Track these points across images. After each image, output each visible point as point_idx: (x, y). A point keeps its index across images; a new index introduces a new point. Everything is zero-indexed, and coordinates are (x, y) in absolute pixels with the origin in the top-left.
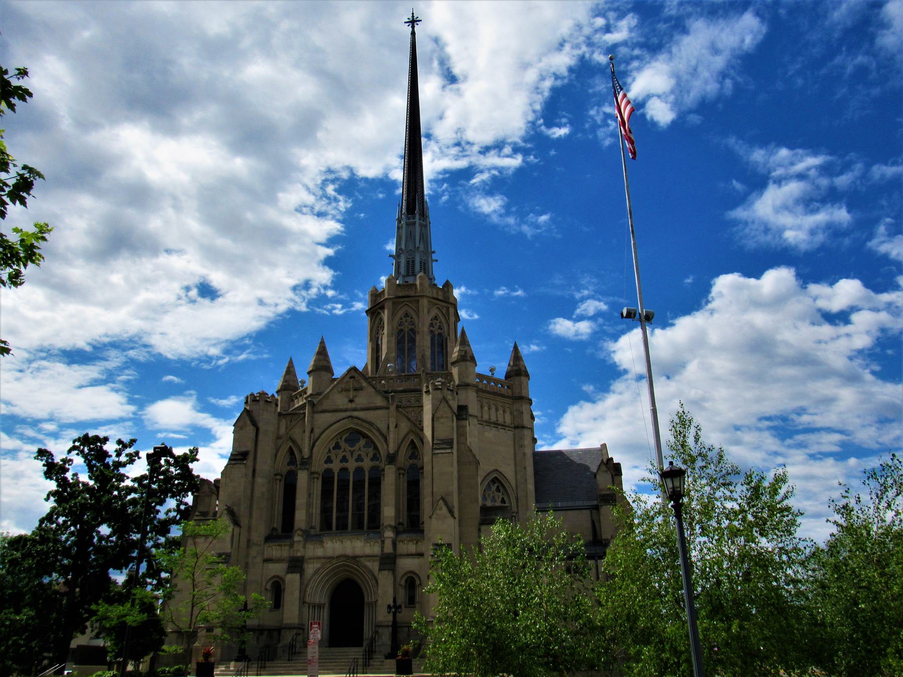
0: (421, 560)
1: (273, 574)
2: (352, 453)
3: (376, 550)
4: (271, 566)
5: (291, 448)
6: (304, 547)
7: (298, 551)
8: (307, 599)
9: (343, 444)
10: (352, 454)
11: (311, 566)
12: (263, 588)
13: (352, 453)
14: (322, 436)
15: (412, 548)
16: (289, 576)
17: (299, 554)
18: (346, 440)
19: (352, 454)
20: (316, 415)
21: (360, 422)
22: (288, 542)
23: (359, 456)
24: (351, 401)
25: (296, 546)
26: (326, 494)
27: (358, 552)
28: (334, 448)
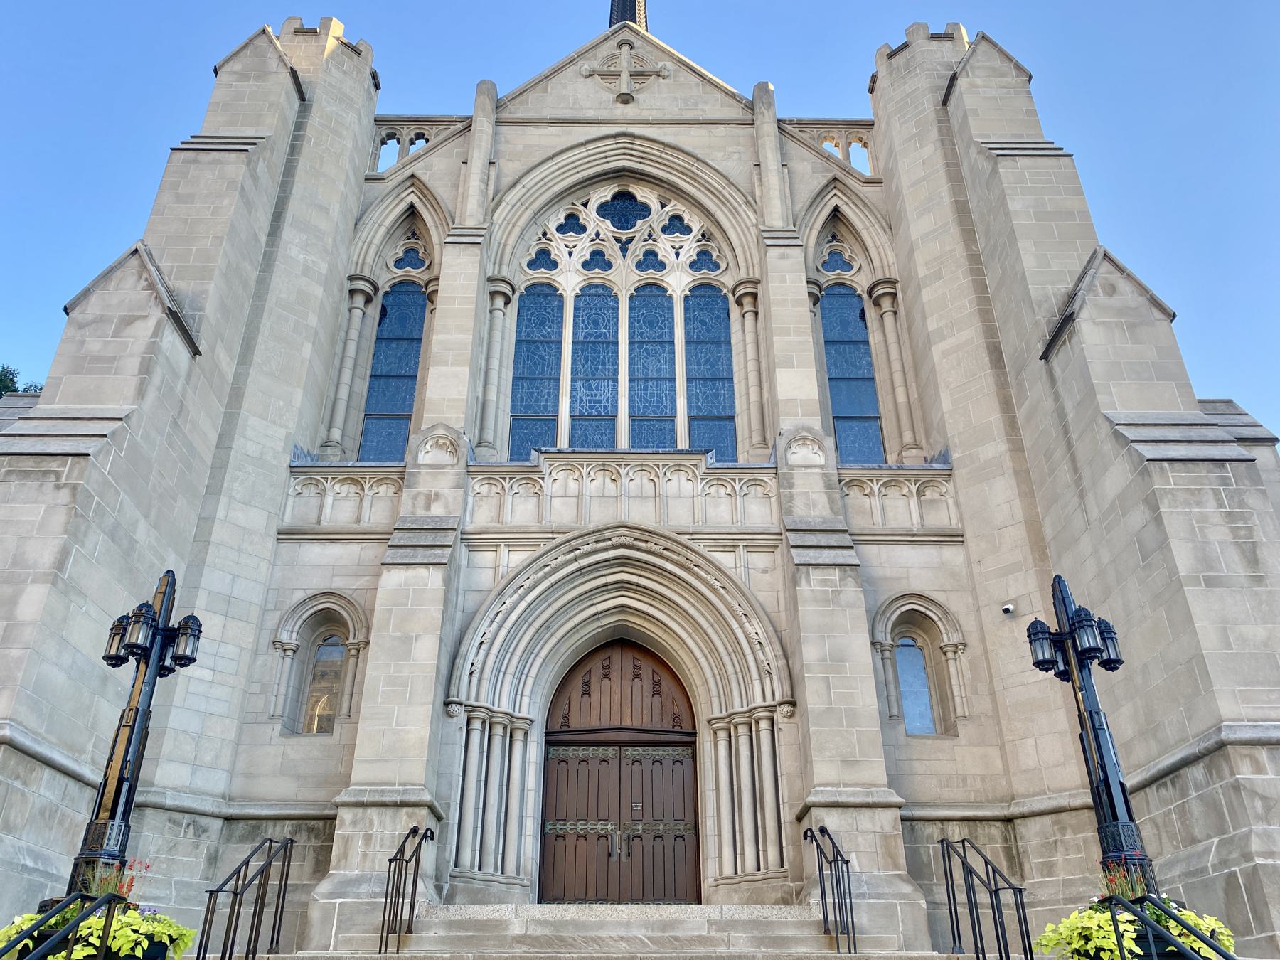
0: (951, 554)
1: (319, 583)
2: (624, 246)
3: (758, 512)
4: (314, 552)
5: (412, 212)
6: (461, 485)
7: (431, 498)
8: (463, 691)
9: (590, 217)
10: (624, 250)
11: (486, 557)
12: (265, 640)
13: (624, 246)
14: (525, 181)
15: (900, 509)
16: (392, 578)
17: (437, 510)
18: (603, 210)
19: (624, 250)
20: (504, 129)
21: (654, 150)
22: (390, 468)
23: (651, 254)
24: (626, 99)
25: (425, 483)
26: (534, 350)
27: (680, 516)
28: (561, 229)
